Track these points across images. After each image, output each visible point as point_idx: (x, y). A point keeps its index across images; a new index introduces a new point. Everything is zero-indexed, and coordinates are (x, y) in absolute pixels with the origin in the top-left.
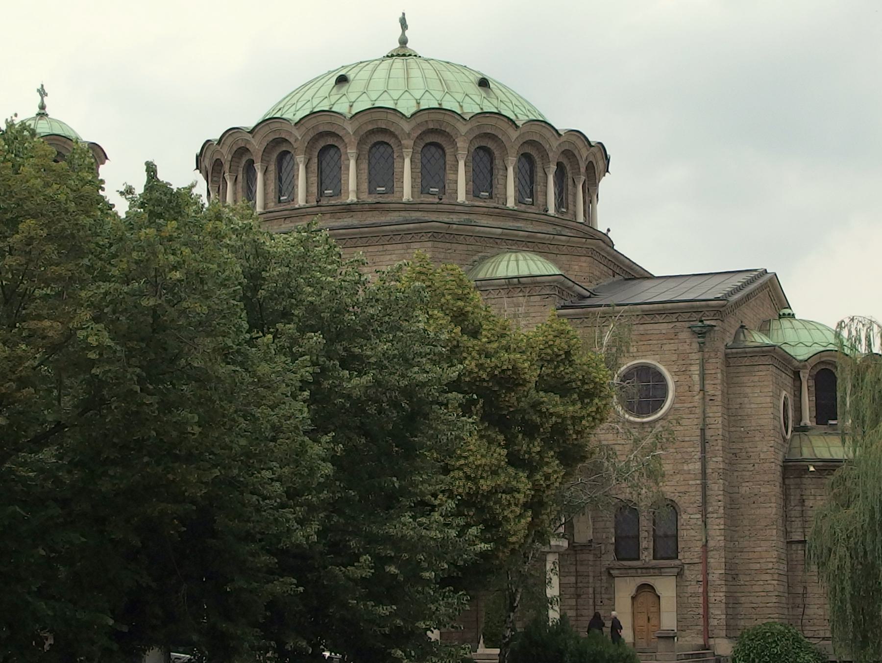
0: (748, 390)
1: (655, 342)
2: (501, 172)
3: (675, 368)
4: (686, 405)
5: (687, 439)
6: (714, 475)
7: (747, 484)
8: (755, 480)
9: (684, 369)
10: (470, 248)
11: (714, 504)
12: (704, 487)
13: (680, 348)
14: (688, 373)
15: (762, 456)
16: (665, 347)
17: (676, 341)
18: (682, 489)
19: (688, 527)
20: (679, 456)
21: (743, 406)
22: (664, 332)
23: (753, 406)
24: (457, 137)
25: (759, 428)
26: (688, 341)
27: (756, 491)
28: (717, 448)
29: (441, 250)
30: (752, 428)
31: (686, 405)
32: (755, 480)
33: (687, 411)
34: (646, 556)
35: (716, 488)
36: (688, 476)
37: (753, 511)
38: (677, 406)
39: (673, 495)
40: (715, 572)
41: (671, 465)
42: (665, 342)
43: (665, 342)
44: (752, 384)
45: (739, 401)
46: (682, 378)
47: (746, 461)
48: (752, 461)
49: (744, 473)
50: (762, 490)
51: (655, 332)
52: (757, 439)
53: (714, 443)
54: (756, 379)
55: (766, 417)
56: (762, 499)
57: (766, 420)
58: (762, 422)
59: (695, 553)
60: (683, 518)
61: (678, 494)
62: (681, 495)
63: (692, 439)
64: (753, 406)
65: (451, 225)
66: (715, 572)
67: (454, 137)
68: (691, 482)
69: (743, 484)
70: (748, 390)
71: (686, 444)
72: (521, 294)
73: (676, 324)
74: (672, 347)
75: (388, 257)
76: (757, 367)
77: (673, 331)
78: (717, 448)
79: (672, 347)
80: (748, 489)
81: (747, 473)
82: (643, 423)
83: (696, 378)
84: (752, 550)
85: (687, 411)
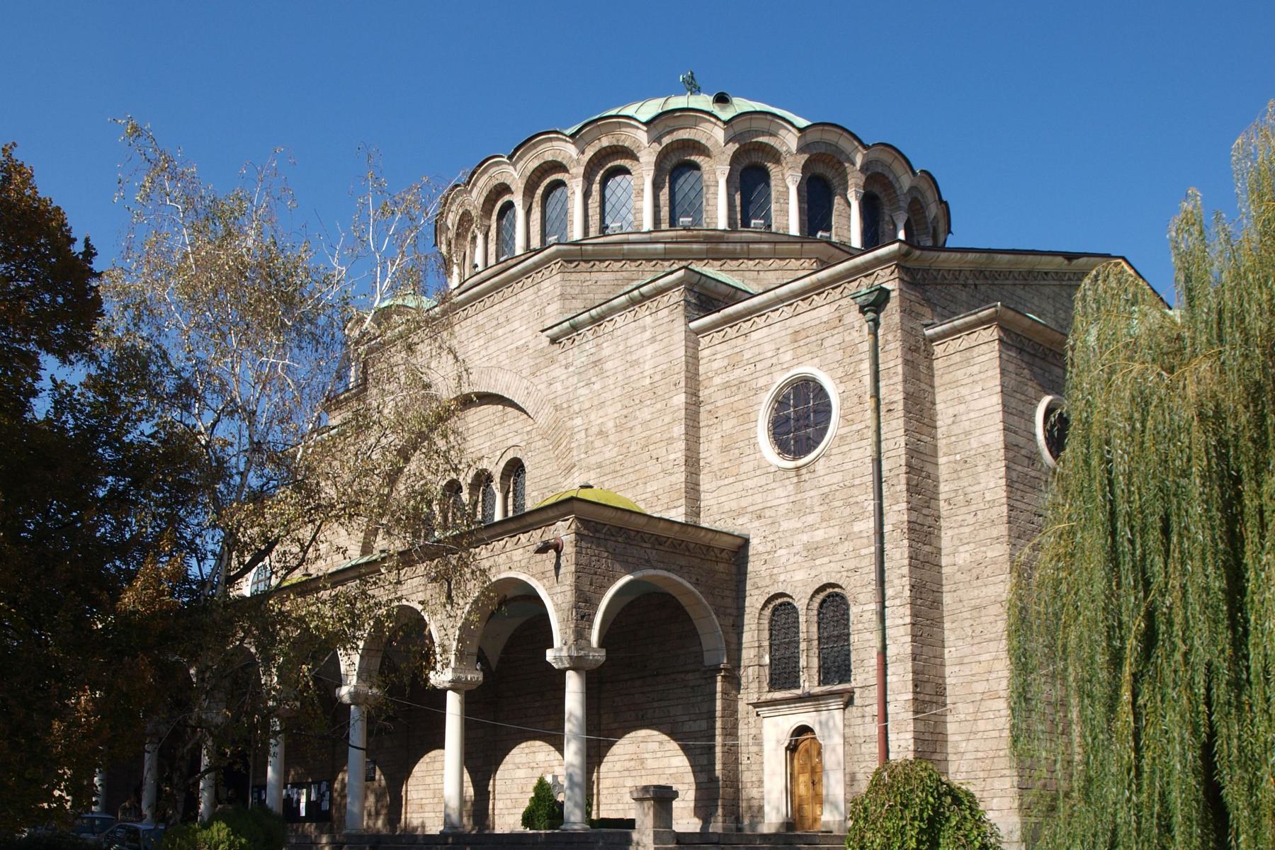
0: (964, 391)
1: (813, 338)
2: (712, 190)
3: (840, 373)
4: (855, 427)
5: (857, 482)
6: (895, 534)
7: (967, 547)
8: (977, 539)
9: (852, 371)
10: (619, 275)
11: (897, 582)
12: (881, 552)
13: (847, 339)
14: (858, 375)
15: (988, 497)
16: (827, 343)
17: (841, 329)
18: (851, 564)
19: (860, 626)
20: (847, 511)
21: (958, 419)
22: (825, 319)
23: (972, 415)
24: (639, 151)
25: (981, 450)
26: (857, 325)
27: (979, 557)
28: (898, 488)
29: (575, 283)
30: (973, 452)
31: (855, 427)
32: (977, 539)
33: (856, 437)
34: (809, 682)
35: (898, 556)
36: (858, 542)
37: (976, 592)
38: (842, 431)
39: (839, 575)
40: (899, 698)
41: (837, 527)
42: (826, 334)
43: (826, 334)
44: (971, 379)
45: (951, 411)
46: (850, 385)
47: (964, 510)
48: (973, 508)
49: (963, 530)
50: (989, 554)
51: (814, 323)
52: (980, 469)
53: (895, 482)
54: (976, 369)
55: (992, 429)
56: (989, 571)
57: (991, 435)
58: (986, 439)
59: (871, 669)
60: (854, 610)
61: (845, 574)
62: (850, 574)
63: (864, 479)
64: (972, 415)
65: (583, 247)
66: (899, 698)
67: (635, 151)
68: (862, 553)
69: (961, 549)
70: (964, 391)
71: (855, 491)
72: (647, 313)
73: (841, 302)
74: (837, 339)
75: (520, 309)
76: (976, 348)
77: (837, 314)
78: (898, 488)
79: (837, 339)
80: (967, 555)
81: (967, 530)
82: (798, 468)
83: (868, 380)
84: (977, 658)
85: (856, 437)
